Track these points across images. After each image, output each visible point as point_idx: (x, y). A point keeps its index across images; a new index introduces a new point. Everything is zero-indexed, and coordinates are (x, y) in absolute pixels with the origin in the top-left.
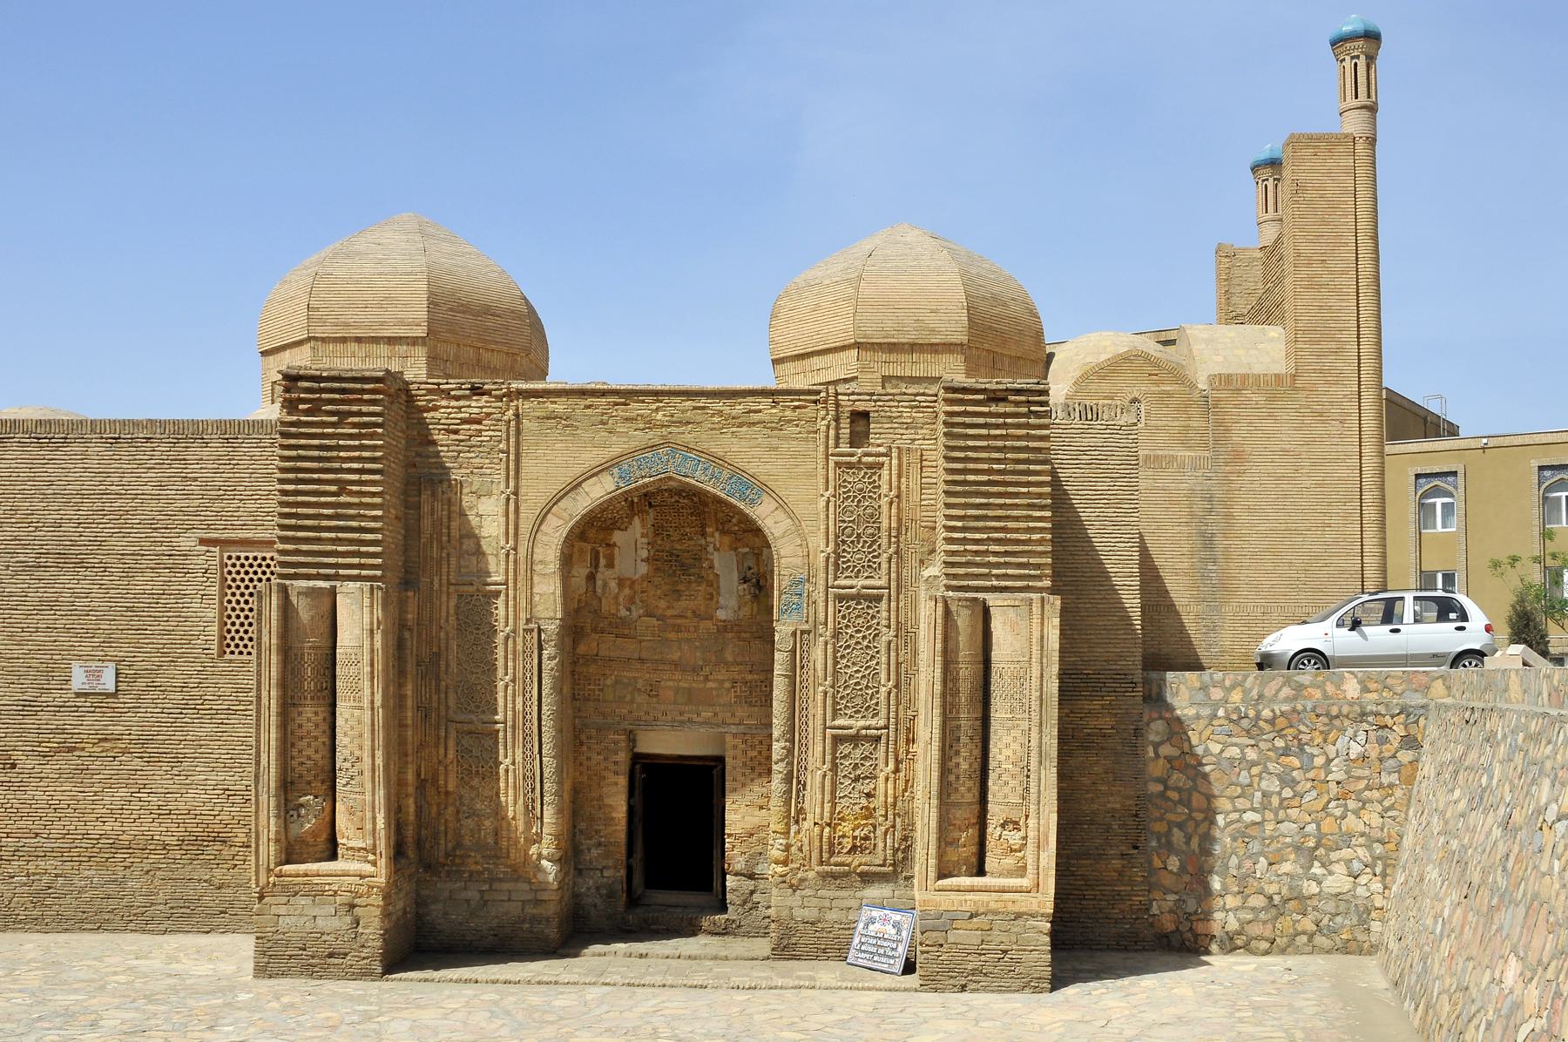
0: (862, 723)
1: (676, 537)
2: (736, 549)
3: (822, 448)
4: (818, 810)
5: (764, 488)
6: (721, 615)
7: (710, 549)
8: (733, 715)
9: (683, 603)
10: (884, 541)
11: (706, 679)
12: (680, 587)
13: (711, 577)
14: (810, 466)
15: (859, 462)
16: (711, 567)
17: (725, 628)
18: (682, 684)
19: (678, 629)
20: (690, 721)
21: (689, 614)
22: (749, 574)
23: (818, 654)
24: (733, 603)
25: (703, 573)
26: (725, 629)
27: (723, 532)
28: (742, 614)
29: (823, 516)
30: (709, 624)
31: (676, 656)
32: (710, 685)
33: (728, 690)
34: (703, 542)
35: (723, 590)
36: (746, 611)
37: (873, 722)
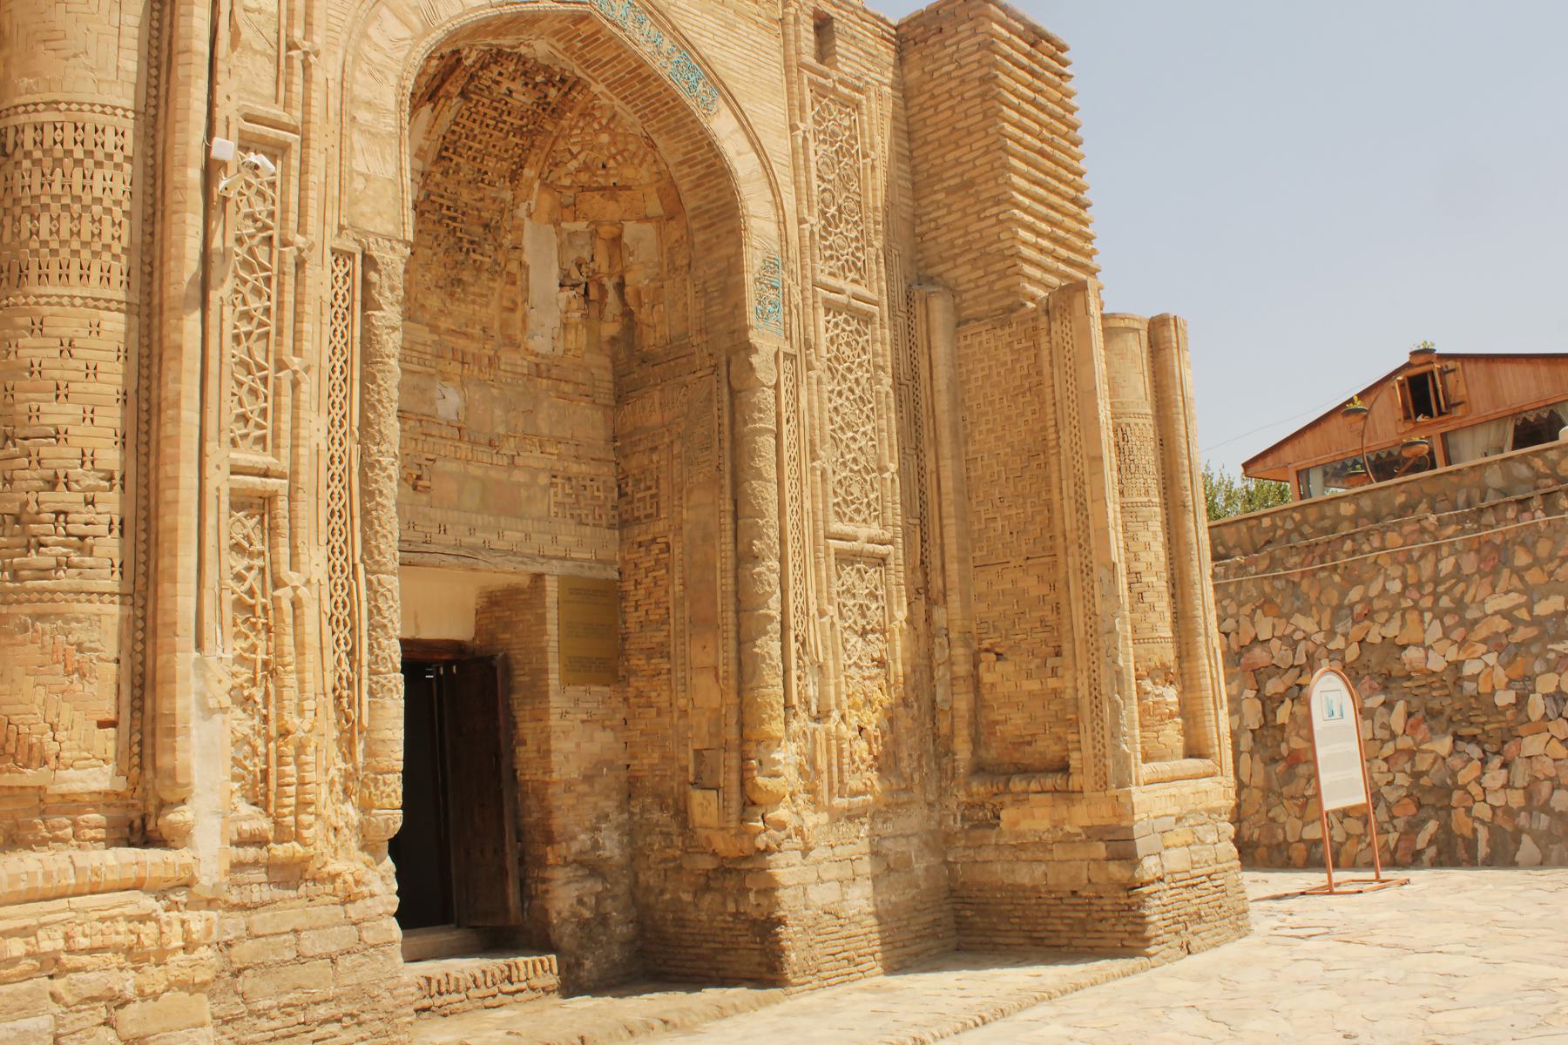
0: (864, 532)
1: (467, 171)
2: (556, 223)
5: (719, 86)
6: (541, 343)
7: (522, 212)
8: (555, 540)
12: (466, 276)
13: (513, 267)
18: (474, 470)
21: (477, 331)
24: (553, 320)
27: (546, 186)
30: (516, 357)
32: (519, 476)
33: (546, 489)
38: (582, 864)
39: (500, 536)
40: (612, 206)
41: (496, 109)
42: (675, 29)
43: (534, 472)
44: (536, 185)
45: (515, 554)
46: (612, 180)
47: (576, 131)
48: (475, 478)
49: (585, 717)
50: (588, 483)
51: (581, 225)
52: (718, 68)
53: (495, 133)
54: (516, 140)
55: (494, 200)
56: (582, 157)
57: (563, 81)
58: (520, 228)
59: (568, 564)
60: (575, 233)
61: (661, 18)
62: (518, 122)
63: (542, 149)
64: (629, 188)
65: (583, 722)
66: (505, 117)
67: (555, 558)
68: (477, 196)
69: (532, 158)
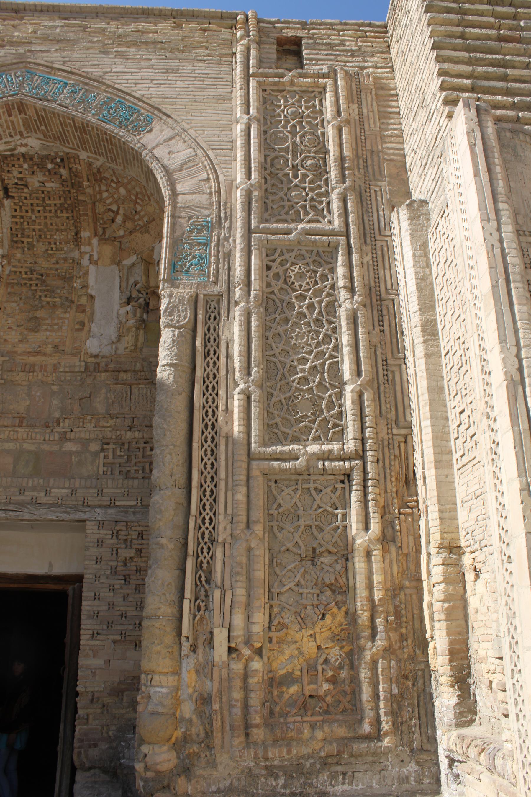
0: (313, 448)
2: (119, 263)
3: (238, 69)
4: (238, 620)
6: (92, 346)
7: (85, 261)
8: (100, 492)
9: (41, 336)
10: (333, 173)
11: (64, 438)
12: (40, 314)
13: (84, 300)
14: (222, 90)
15: (292, 83)
16: (85, 286)
17: (95, 366)
18: (27, 446)
19: (30, 369)
20: (34, 502)
21: (49, 349)
22: (135, 294)
23: (233, 332)
24: (112, 331)
25: (74, 298)
26: (97, 368)
27: (103, 240)
28: (121, 347)
29: (239, 142)
31: (22, 407)
32: (69, 447)
33: (96, 454)
34: (76, 254)
35: (98, 315)
36: (128, 340)
37: (336, 447)
38: (105, 771)
39: (47, 493)
40: (146, 236)
41: (37, 199)
42: (109, 86)
43: (85, 443)
44: (95, 241)
45: (60, 506)
46: (145, 219)
47: (105, 195)
48: (30, 452)
49: (118, 637)
50: (142, 445)
51: (133, 258)
52: (155, 101)
53: (48, 215)
54: (65, 215)
55: (65, 259)
56: (121, 212)
57: (62, 160)
58: (86, 273)
59: (111, 511)
60: (133, 265)
61: (96, 84)
62: (58, 202)
63: (87, 215)
64: (154, 220)
65: (115, 642)
66: (47, 202)
67: (100, 506)
68: (54, 260)
69: (84, 224)
